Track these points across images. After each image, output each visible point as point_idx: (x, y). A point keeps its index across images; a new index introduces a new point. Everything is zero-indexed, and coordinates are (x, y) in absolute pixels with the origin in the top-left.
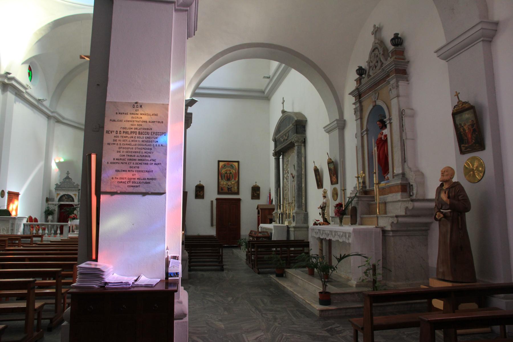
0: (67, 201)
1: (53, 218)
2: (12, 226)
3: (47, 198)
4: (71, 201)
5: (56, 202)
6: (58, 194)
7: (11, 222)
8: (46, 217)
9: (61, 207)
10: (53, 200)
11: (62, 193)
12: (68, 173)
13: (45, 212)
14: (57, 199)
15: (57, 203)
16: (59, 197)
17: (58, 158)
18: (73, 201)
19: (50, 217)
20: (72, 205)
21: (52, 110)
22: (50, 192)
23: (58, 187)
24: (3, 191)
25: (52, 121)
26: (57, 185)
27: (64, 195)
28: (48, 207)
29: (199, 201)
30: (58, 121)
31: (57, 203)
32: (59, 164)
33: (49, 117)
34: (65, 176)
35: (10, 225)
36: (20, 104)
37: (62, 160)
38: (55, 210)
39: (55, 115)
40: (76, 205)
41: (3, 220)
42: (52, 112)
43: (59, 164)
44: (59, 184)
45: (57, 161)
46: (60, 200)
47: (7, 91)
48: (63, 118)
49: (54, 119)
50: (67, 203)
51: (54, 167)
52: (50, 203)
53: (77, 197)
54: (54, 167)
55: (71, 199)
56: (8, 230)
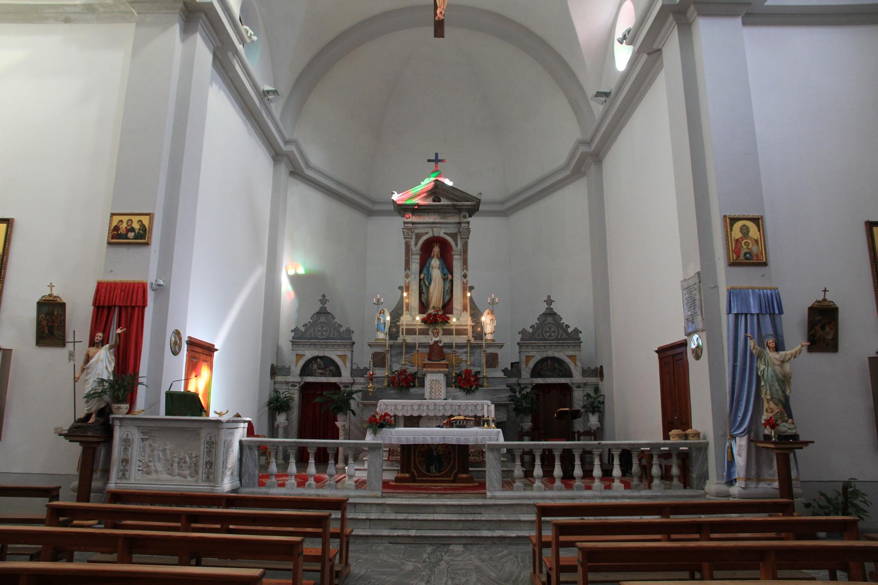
0: (322, 375)
1: (287, 419)
2: (209, 452)
3: (272, 366)
4: (334, 375)
5: (295, 377)
6: (299, 357)
7: (204, 435)
8: (272, 418)
9: (307, 390)
10: (287, 371)
11: (309, 354)
12: (324, 300)
13: (270, 403)
14: (296, 369)
15: (298, 379)
16: (302, 363)
17: (294, 265)
18: (338, 374)
19: (281, 419)
20: (335, 386)
21: (287, 137)
22: (278, 351)
23: (299, 338)
24: (177, 333)
25: (283, 169)
26: (295, 331)
27: (315, 358)
28: (276, 391)
29: (822, 359)
30: (296, 173)
31: (298, 379)
32: (295, 280)
33: (277, 156)
34: (317, 307)
35: (203, 448)
36: (222, 92)
37: (301, 271)
38: (292, 399)
39: (292, 148)
40: (346, 386)
41: (171, 429)
42: (286, 142)
43: (295, 280)
44: (303, 329)
45: (292, 272)
46: (305, 370)
47: (194, 32)
48: (308, 165)
49: (286, 161)
50: (324, 379)
51: (286, 288)
52: (279, 378)
53: (349, 365)
54: (286, 288)
55: (332, 368)
56: (196, 465)
